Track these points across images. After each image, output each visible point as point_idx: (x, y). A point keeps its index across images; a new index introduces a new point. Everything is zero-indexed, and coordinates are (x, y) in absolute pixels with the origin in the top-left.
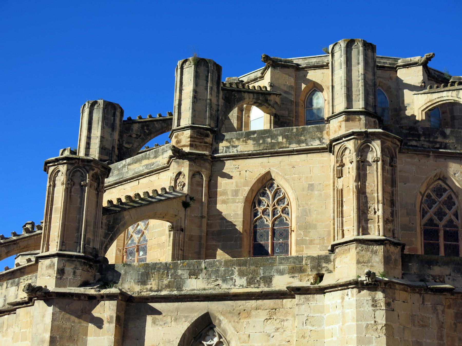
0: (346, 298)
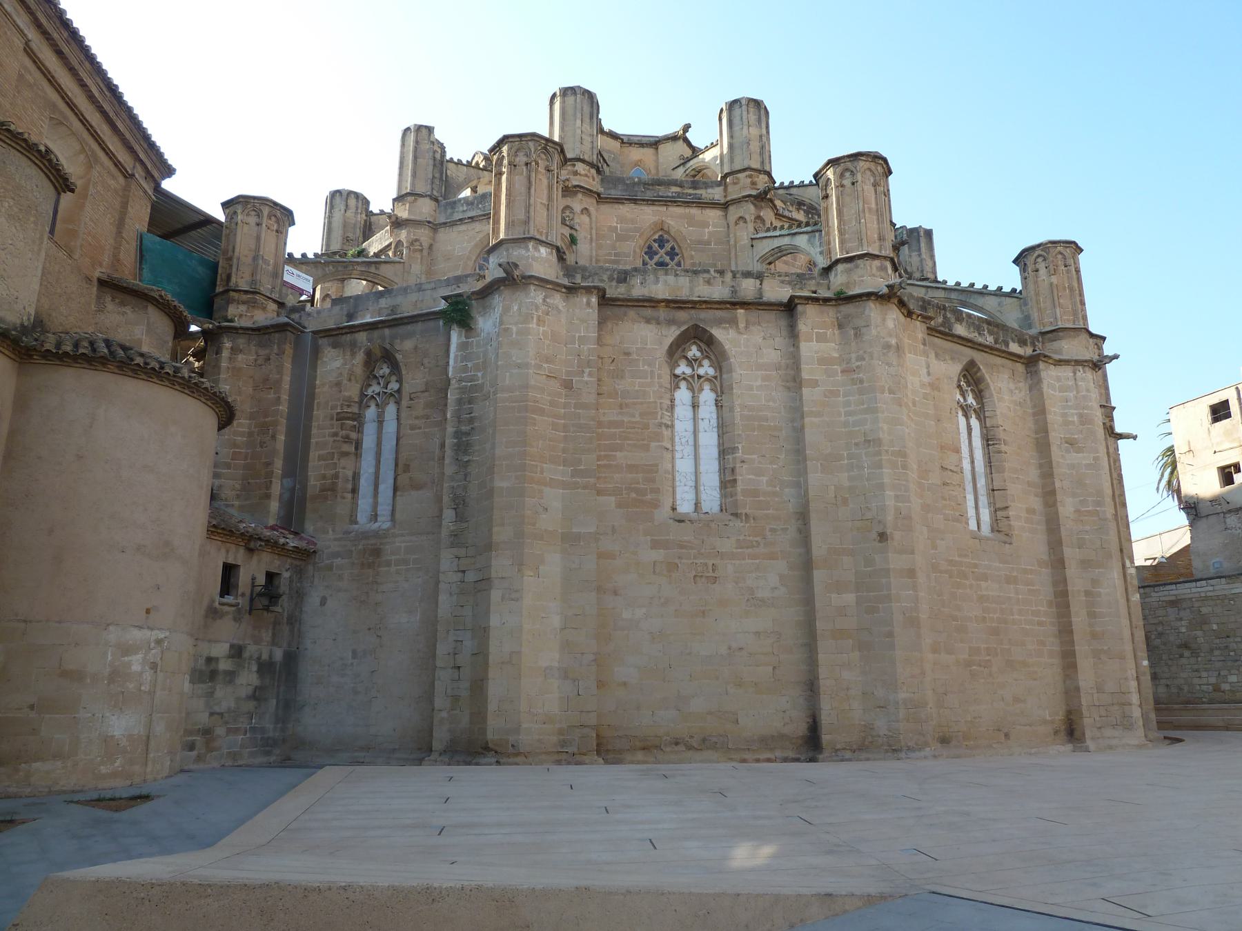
0: (1078, 374)
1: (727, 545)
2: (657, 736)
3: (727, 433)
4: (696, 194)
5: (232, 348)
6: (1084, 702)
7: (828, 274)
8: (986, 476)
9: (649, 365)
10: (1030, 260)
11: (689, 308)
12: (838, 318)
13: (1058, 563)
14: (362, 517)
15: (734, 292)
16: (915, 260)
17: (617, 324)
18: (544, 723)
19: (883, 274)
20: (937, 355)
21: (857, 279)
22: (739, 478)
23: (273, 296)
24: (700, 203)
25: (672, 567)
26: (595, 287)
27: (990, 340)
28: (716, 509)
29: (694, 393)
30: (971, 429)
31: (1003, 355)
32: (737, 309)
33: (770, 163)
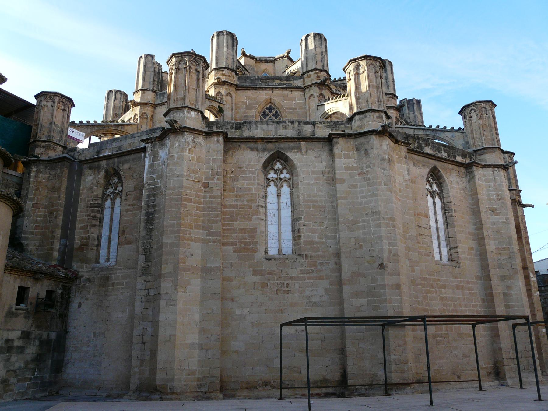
0: (496, 172)
1: (295, 272)
2: (254, 381)
3: (296, 209)
4: (288, 84)
5: (36, 171)
6: (504, 356)
7: (351, 121)
8: (445, 230)
9: (252, 173)
10: (467, 112)
11: (274, 142)
12: (356, 145)
13: (486, 277)
14: (102, 260)
15: (299, 132)
16: (412, 115)
17: (235, 152)
18: (189, 375)
19: (380, 120)
20: (414, 164)
21: (366, 123)
22: (302, 235)
23: (60, 143)
24: (290, 88)
25: (264, 285)
26: (221, 132)
27: (445, 155)
28: (290, 252)
29: (278, 188)
30: (436, 204)
31: (453, 163)
32: (301, 142)
33: (328, 66)
